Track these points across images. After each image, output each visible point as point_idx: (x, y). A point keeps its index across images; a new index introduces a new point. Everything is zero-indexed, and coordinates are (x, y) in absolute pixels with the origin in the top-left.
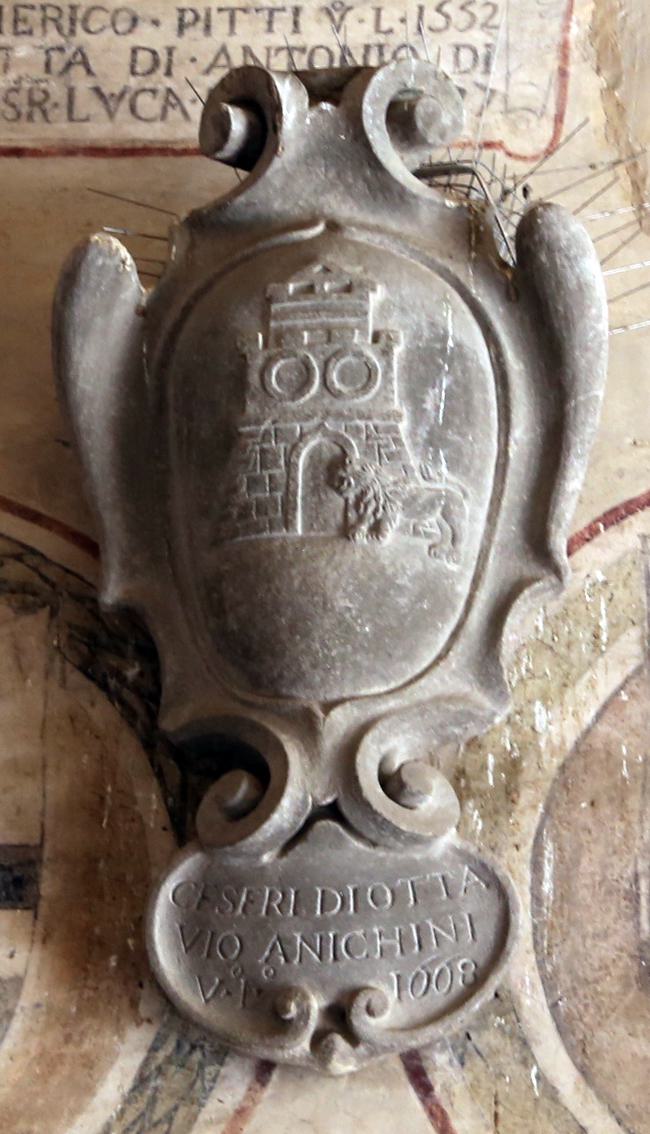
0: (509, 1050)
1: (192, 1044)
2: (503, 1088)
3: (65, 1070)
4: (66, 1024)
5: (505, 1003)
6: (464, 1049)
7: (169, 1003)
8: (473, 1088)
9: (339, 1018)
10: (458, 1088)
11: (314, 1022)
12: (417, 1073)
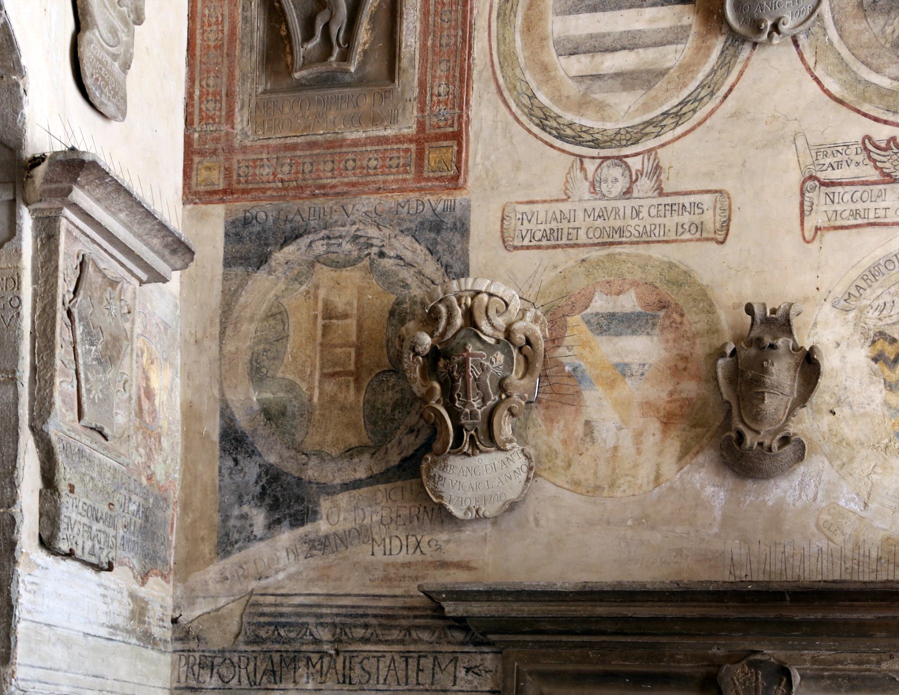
0: (821, 31)
1: (736, 39)
2: (819, 44)
3: (702, 51)
4: (703, 37)
5: (820, 18)
6: (808, 33)
7: (731, 29)
8: (810, 45)
9: (775, 27)
10: (806, 45)
11: (768, 29)
12: (795, 42)
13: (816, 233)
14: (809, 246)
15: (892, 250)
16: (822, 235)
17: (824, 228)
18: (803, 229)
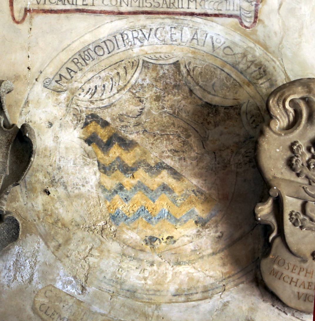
13: (25, 14)
14: (19, 26)
15: (101, 37)
16: (31, 17)
17: (34, 10)
18: (12, 10)
